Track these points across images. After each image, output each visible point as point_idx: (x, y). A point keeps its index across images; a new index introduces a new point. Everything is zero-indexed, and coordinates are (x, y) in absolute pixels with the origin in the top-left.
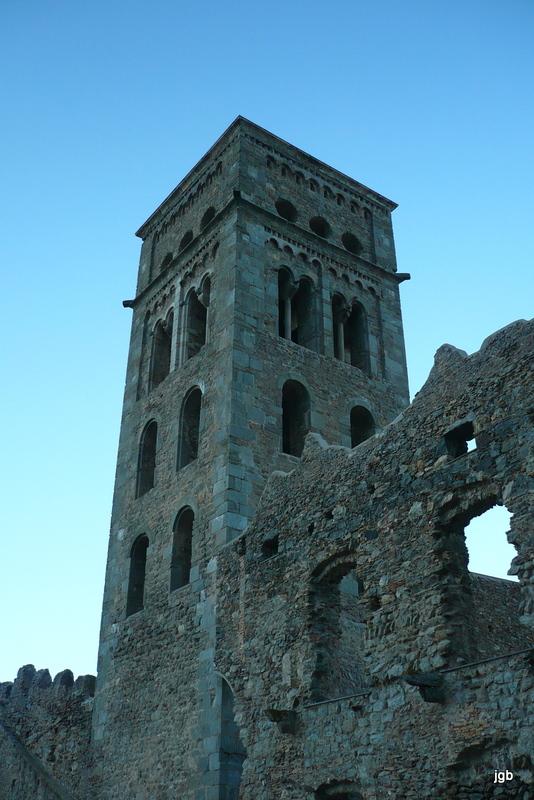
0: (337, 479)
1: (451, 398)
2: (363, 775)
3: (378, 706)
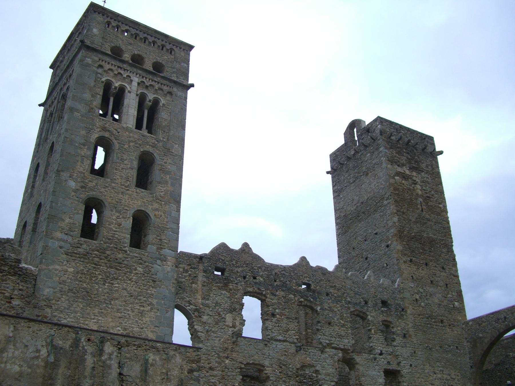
0: (260, 268)
1: (306, 274)
2: (267, 363)
3: (274, 346)
